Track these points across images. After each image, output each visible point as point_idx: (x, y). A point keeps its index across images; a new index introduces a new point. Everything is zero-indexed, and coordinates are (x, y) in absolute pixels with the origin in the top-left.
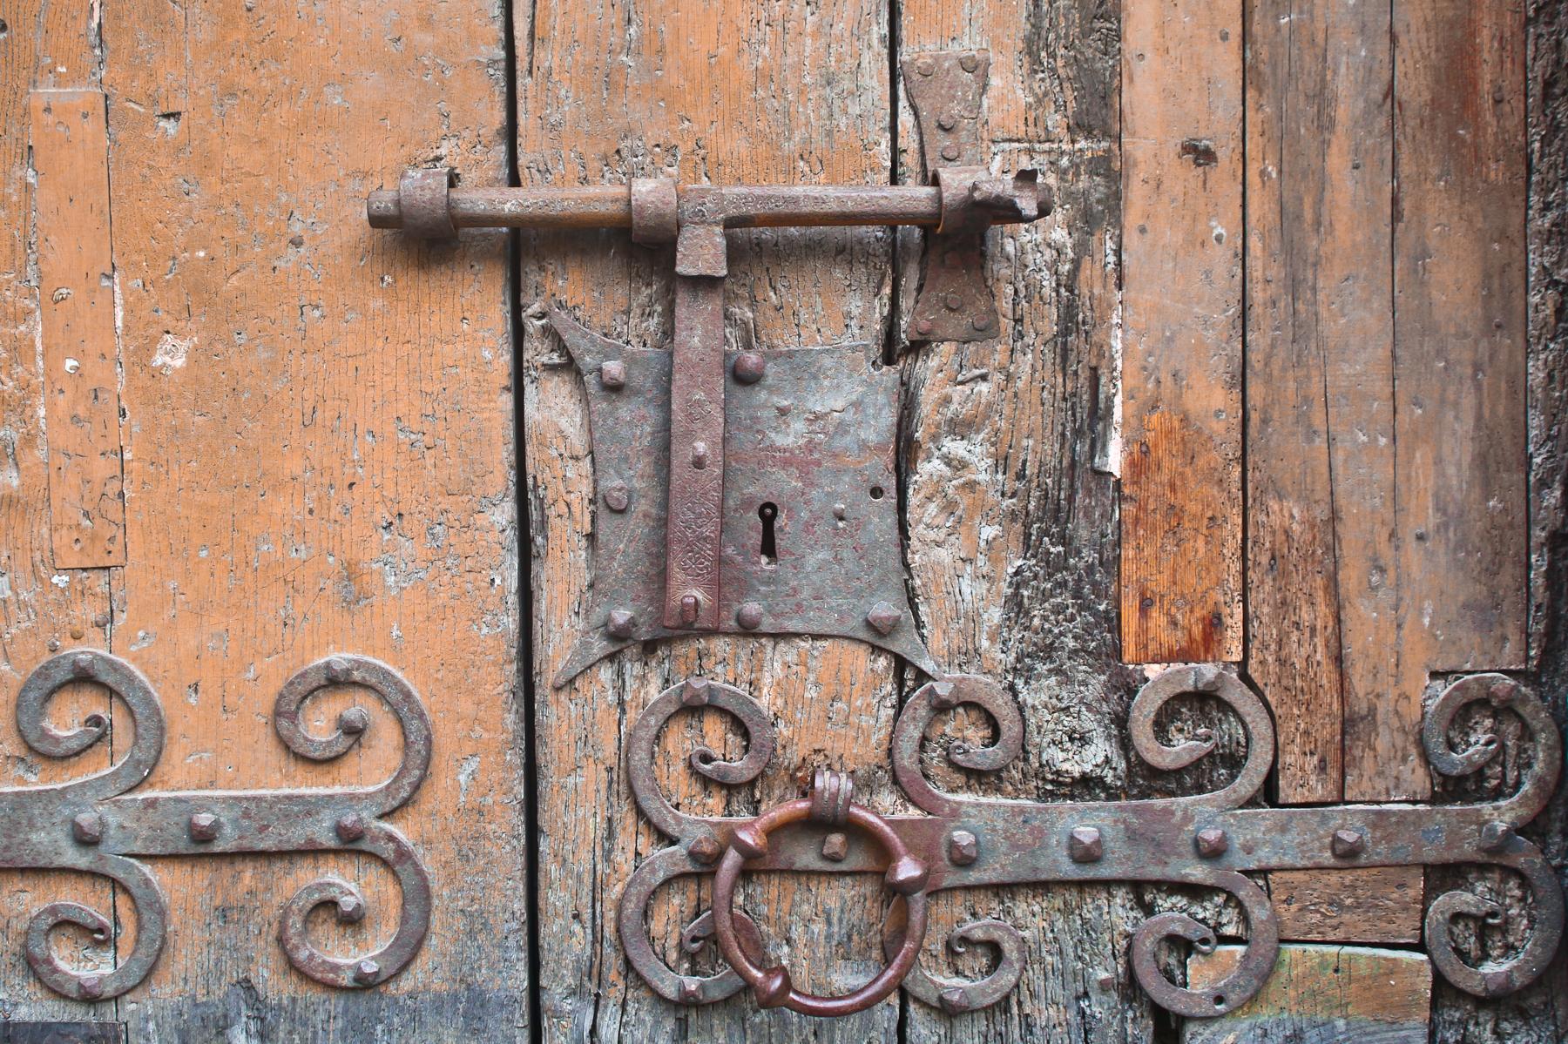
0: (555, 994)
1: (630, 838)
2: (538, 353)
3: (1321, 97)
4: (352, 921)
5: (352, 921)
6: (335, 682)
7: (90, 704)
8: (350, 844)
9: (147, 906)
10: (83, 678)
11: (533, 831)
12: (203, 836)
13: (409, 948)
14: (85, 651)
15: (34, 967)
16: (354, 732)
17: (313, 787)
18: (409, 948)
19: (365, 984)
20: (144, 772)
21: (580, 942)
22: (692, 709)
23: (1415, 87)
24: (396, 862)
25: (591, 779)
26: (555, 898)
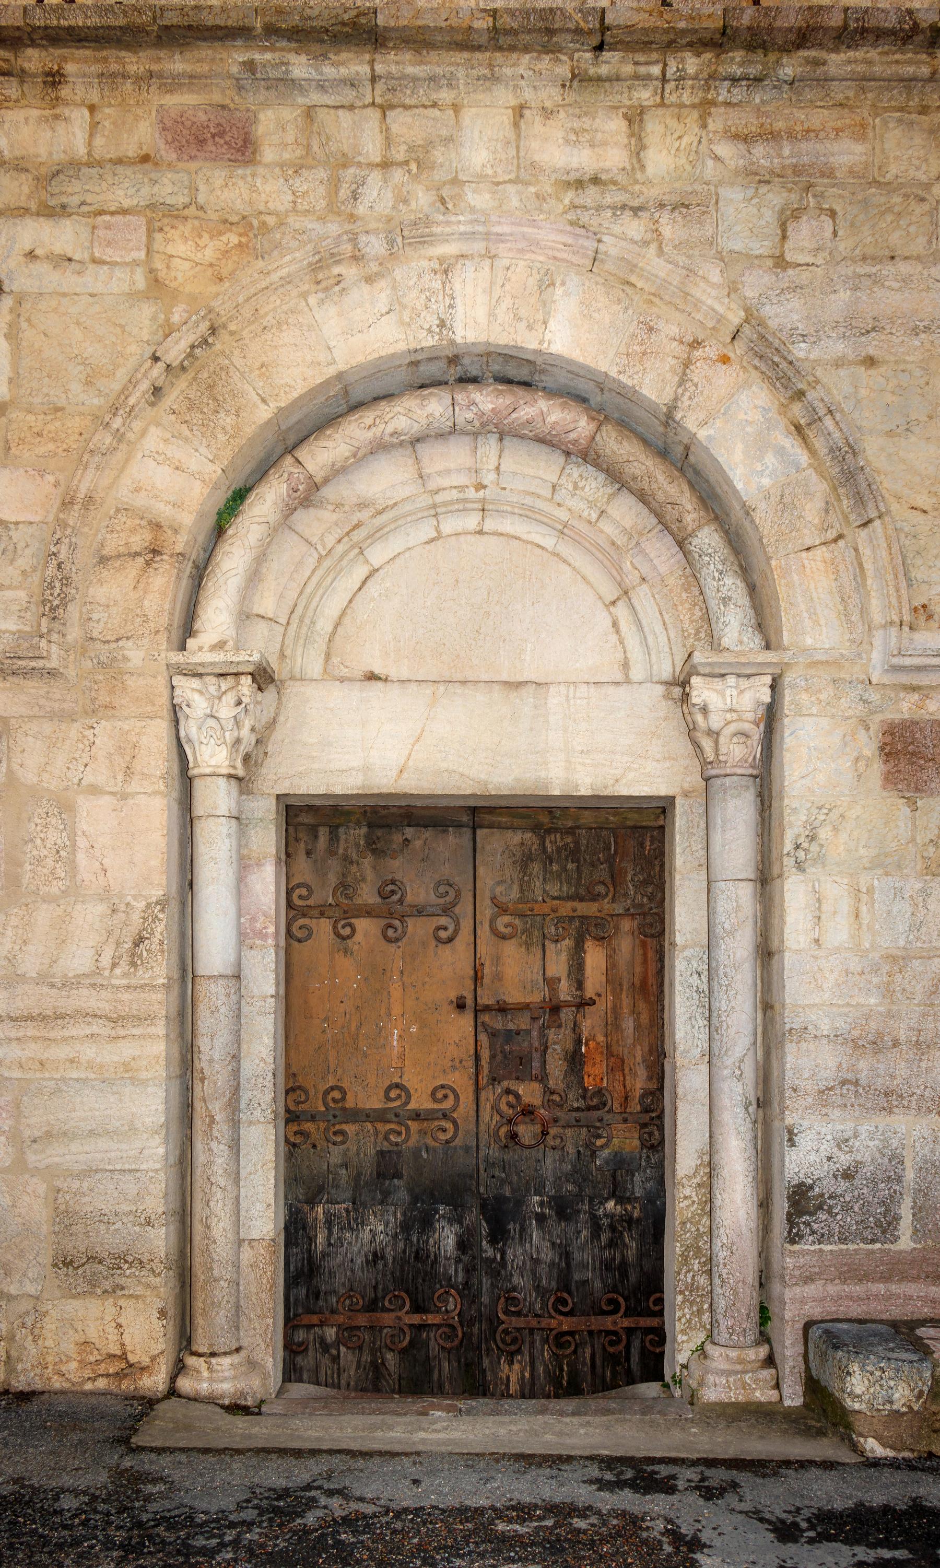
0: (481, 1145)
1: (497, 1118)
2: (480, 1029)
3: (621, 985)
4: (444, 1130)
5: (444, 1130)
6: (443, 1087)
7: (398, 1091)
8: (445, 1116)
9: (408, 1129)
10: (397, 1086)
11: (478, 1116)
12: (418, 1115)
13: (455, 1136)
14: (396, 1080)
15: (386, 1138)
16: (446, 1096)
17: (436, 1106)
18: (455, 1136)
19: (447, 1142)
20: (407, 1103)
21: (486, 1136)
22: (508, 1092)
23: (637, 982)
24: (455, 1122)
25: (488, 1107)
26: (482, 1127)
